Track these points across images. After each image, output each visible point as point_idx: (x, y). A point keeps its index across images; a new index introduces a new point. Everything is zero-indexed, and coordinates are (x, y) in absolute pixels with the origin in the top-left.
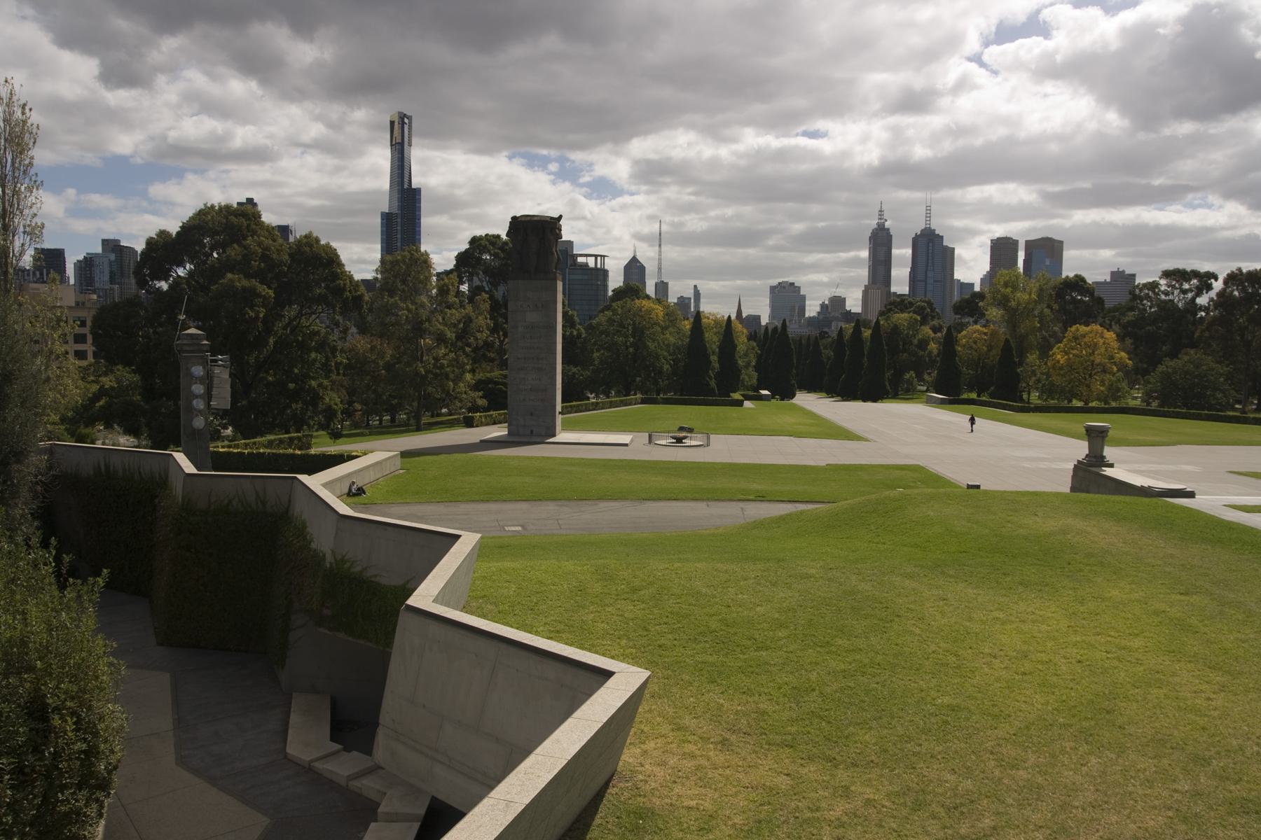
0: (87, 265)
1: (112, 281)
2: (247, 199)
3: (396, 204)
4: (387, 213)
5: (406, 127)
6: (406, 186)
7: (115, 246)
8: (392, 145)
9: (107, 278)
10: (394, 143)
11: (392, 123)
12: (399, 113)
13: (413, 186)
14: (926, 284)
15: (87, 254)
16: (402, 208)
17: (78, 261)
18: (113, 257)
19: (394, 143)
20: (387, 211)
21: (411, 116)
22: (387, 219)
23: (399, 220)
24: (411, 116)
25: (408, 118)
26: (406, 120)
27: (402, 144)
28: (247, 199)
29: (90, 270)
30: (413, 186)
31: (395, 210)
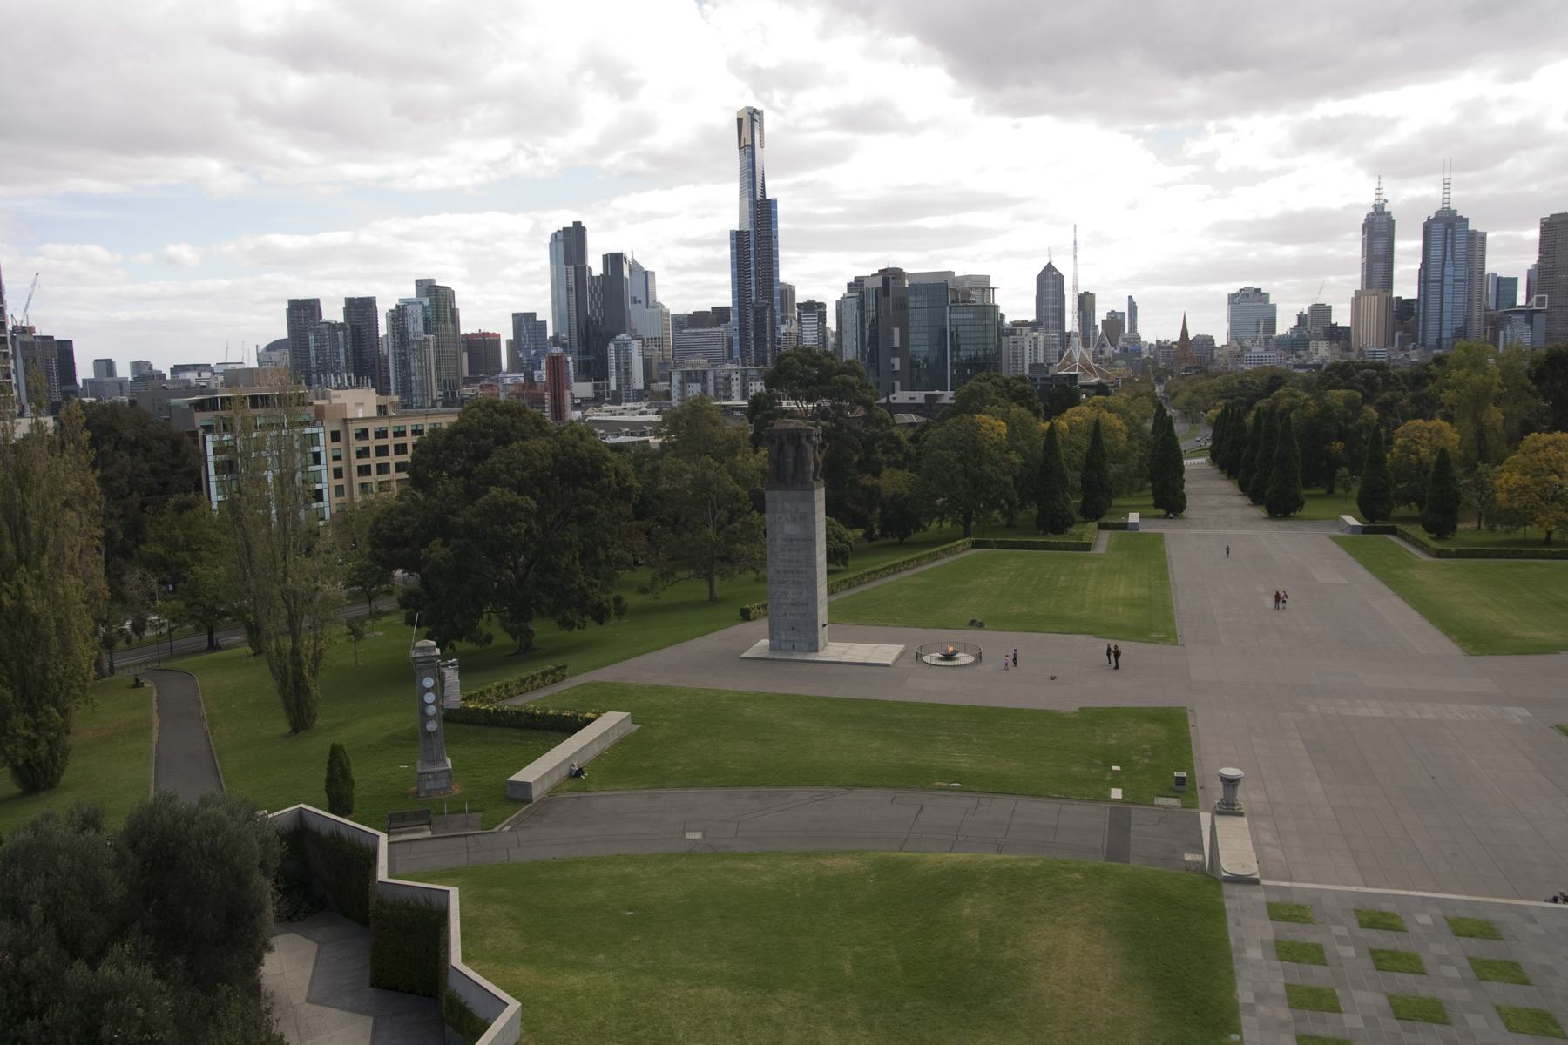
0: (399, 314)
1: (427, 331)
2: (574, 223)
3: (748, 220)
4: (737, 232)
5: (757, 124)
6: (759, 197)
7: (430, 286)
8: (740, 148)
9: (421, 328)
10: (742, 145)
11: (740, 121)
12: (747, 108)
13: (768, 198)
14: (1442, 286)
15: (401, 300)
16: (755, 224)
17: (390, 311)
18: (427, 302)
19: (742, 145)
20: (737, 229)
21: (762, 111)
22: (739, 239)
23: (752, 239)
24: (762, 111)
25: (758, 114)
26: (756, 117)
27: (752, 146)
28: (574, 223)
29: (403, 320)
30: (768, 198)
31: (747, 228)
